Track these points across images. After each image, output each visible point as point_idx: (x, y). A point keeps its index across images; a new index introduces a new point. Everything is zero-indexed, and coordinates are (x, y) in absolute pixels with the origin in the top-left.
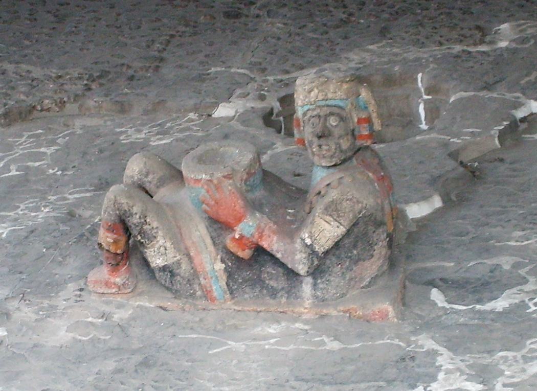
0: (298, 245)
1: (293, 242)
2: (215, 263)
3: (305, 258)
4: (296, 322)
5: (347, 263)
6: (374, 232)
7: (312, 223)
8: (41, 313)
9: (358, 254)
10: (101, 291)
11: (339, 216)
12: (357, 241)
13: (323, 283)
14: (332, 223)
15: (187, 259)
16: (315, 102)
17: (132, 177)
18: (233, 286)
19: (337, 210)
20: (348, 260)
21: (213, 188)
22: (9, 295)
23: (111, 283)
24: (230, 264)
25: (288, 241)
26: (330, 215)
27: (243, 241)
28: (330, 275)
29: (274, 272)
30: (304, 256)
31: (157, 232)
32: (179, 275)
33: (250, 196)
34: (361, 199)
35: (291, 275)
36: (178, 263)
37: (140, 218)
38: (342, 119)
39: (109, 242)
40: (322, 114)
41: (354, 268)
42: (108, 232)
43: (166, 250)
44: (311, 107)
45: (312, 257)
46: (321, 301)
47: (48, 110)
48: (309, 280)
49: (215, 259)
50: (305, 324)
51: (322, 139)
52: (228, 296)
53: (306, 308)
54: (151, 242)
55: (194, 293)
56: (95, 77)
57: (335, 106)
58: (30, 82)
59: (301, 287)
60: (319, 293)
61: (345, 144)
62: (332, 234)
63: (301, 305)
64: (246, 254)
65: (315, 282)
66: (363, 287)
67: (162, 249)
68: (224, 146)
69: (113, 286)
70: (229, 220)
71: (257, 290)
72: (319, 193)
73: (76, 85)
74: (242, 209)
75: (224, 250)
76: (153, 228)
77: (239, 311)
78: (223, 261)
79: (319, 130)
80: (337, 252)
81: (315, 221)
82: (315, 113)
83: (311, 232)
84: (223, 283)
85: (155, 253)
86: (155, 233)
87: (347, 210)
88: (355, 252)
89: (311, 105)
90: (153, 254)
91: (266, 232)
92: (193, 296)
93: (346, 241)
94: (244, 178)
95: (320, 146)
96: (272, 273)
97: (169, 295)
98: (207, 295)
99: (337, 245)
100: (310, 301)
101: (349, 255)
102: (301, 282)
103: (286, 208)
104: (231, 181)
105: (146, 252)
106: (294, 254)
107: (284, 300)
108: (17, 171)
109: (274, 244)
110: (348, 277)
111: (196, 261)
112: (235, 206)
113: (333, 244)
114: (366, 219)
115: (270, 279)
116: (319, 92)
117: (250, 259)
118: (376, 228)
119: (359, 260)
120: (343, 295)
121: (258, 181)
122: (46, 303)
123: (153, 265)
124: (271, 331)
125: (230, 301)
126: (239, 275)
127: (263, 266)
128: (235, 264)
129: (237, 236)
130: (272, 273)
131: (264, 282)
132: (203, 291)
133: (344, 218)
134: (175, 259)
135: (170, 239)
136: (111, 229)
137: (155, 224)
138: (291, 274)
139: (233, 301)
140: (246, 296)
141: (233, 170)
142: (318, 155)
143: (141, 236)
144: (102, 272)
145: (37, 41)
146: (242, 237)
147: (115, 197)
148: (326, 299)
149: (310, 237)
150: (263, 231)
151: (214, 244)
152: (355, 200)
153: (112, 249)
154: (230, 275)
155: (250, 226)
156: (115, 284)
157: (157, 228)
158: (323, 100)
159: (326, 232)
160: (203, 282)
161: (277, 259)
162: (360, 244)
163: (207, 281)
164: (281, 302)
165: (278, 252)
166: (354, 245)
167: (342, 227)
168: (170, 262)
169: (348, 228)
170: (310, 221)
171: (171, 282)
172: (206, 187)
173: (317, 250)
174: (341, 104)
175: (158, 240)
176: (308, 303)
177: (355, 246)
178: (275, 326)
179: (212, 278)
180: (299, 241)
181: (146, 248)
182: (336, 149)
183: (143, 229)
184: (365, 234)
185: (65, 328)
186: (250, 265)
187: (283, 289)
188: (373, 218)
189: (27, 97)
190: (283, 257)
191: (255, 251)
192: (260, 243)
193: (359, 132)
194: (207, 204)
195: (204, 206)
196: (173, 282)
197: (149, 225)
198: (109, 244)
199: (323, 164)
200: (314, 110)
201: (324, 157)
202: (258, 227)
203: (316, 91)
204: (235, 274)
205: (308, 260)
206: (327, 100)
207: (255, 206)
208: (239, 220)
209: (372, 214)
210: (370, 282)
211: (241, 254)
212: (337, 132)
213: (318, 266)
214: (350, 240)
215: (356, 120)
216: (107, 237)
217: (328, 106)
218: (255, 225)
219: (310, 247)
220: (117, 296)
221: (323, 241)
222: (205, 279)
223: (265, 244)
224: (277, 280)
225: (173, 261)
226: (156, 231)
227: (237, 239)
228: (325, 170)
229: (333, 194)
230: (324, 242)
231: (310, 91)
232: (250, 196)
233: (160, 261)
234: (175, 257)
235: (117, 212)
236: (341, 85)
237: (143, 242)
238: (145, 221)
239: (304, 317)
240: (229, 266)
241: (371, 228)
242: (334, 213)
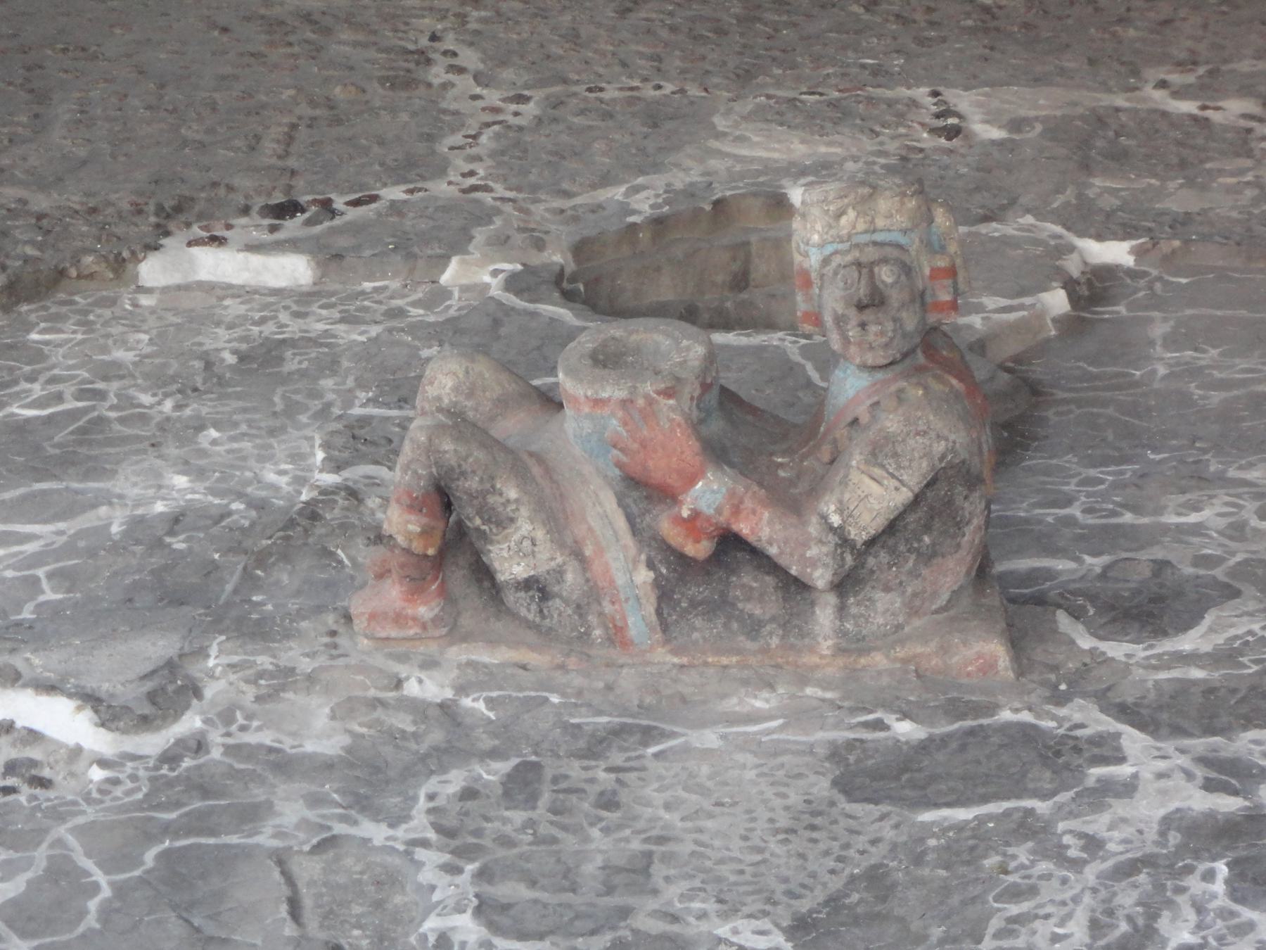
0: (814, 529)
1: (805, 524)
2: (635, 568)
3: (827, 555)
4: (806, 685)
5: (911, 563)
6: (966, 498)
7: (844, 483)
8: (262, 682)
9: (934, 544)
10: (383, 634)
11: (899, 467)
12: (932, 518)
13: (858, 604)
14: (886, 482)
15: (576, 563)
16: (850, 236)
17: (439, 398)
18: (670, 615)
19: (895, 455)
20: (913, 557)
21: (637, 416)
22: (182, 648)
23: (406, 617)
24: (664, 571)
25: (793, 520)
26: (883, 466)
27: (698, 524)
28: (873, 588)
29: (755, 585)
30: (825, 549)
31: (517, 509)
32: (561, 597)
33: (704, 430)
34: (946, 432)
35: (793, 588)
36: (559, 573)
37: (482, 480)
38: (907, 270)
39: (410, 533)
40: (864, 259)
42: (410, 513)
43: (534, 544)
44: (840, 247)
45: (842, 553)
47: (91, 276)
48: (832, 599)
49: (635, 562)
50: (824, 689)
51: (867, 311)
52: (658, 636)
53: (822, 657)
54: (504, 528)
56: (169, 210)
57: (890, 244)
58: (33, 221)
59: (813, 613)
60: (849, 626)
61: (910, 321)
62: (885, 504)
63: (812, 650)
64: (699, 549)
65: (842, 603)
66: (937, 612)
67: (527, 543)
68: (637, 331)
69: (410, 623)
70: (669, 481)
71: (720, 622)
72: (855, 421)
73: (136, 225)
74: (697, 458)
75: (653, 543)
77: (682, 666)
78: (651, 565)
79: (863, 291)
80: (891, 542)
82: (849, 258)
83: (841, 502)
84: (650, 609)
86: (513, 511)
87: (916, 455)
88: (927, 539)
89: (842, 242)
90: (505, 554)
91: (748, 504)
92: (585, 637)
93: (911, 518)
94: (696, 394)
95: (863, 325)
97: (531, 636)
98: (617, 635)
99: (892, 527)
100: (830, 643)
101: (916, 545)
102: (813, 604)
103: (772, 454)
104: (671, 402)
105: (490, 551)
106: (805, 545)
107: (775, 641)
108: (78, 399)
110: (910, 590)
111: (597, 567)
112: (682, 453)
113: (886, 523)
115: (749, 599)
116: (857, 217)
117: (709, 560)
119: (934, 555)
121: (714, 403)
122: (264, 661)
123: (501, 577)
124: (759, 704)
125: (663, 646)
126: (683, 594)
127: (733, 572)
128: (675, 570)
129: (685, 513)
130: (752, 588)
131: (733, 605)
132: (606, 628)
134: (553, 564)
135: (544, 525)
136: (414, 506)
137: (513, 494)
139: (668, 647)
140: (696, 635)
141: (678, 379)
142: (860, 344)
143: (482, 518)
144: (393, 593)
145: (11, 141)
146: (696, 514)
147: (430, 440)
148: (864, 637)
149: (840, 511)
150: (741, 502)
151: (634, 530)
152: (933, 434)
153: (417, 547)
154: (664, 593)
155: (713, 492)
156: (414, 619)
157: (517, 501)
158: (866, 232)
159: (871, 500)
160: (608, 608)
161: (768, 558)
162: (937, 524)
163: (617, 607)
164: (768, 645)
165: (771, 545)
167: (904, 489)
168: (542, 569)
169: (917, 490)
170: (838, 479)
171: (541, 611)
172: (620, 414)
173: (852, 537)
174: (903, 240)
176: (826, 646)
177: (927, 528)
178: (765, 694)
179: (627, 600)
180: (814, 519)
181: (491, 542)
182: (894, 331)
183: (487, 504)
184: (950, 502)
185: (327, 710)
186: (708, 573)
187: (773, 619)
188: (964, 470)
189: (42, 251)
190: (781, 553)
191: (718, 544)
192: (735, 527)
193: (934, 295)
194: (622, 450)
195: (615, 452)
196: (545, 611)
198: (409, 536)
199: (870, 362)
200: (848, 251)
201: (871, 348)
202: (732, 494)
203: (851, 214)
204: (674, 592)
205: (834, 558)
206: (874, 231)
207: (717, 453)
208: (691, 481)
209: (963, 462)
210: (949, 601)
211: (691, 549)
212: (895, 297)
214: (918, 515)
215: (927, 271)
216: (408, 522)
217: (875, 243)
218: (724, 490)
219: (839, 532)
220: (418, 643)
221: (866, 519)
222: (613, 603)
223: (743, 528)
224: (761, 599)
225: (547, 567)
226: (514, 507)
227: (684, 520)
228: (865, 375)
230: (866, 524)
231: (840, 214)
232: (704, 430)
233: (521, 568)
234: (552, 559)
236: (903, 204)
237: (484, 532)
238: (493, 487)
239: (818, 675)
240: (661, 574)
241: (960, 490)
242: (891, 461)
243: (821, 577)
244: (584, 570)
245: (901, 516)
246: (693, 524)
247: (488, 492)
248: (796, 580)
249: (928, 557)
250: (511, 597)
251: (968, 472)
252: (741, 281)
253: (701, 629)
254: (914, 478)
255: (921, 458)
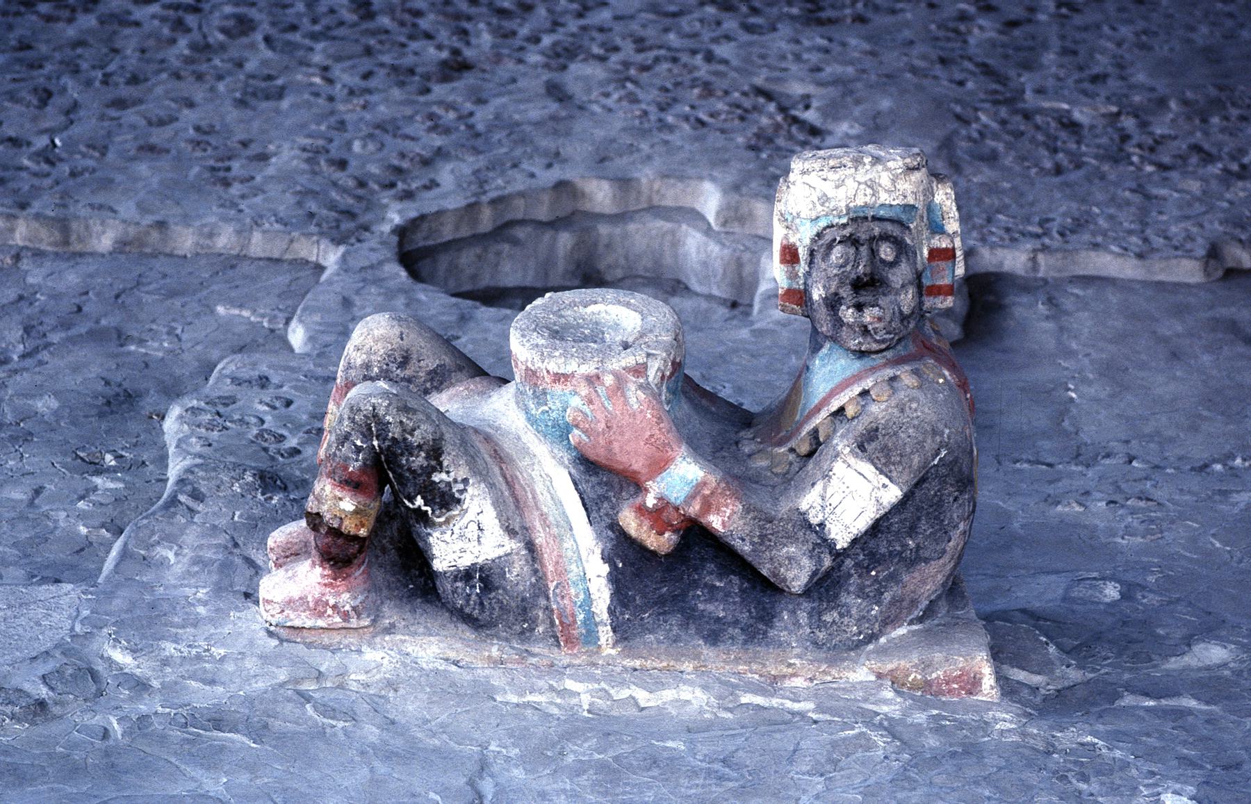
6: (956, 499)
7: (827, 476)
9: (918, 547)
10: (297, 623)
12: (919, 519)
34: (941, 426)
41: (906, 578)
44: (836, 221)
55: (532, 630)
67: (474, 527)
76: (455, 481)
81: (835, 470)
85: (455, 536)
96: (714, 586)
114: (943, 471)
118: (961, 492)
120: (872, 638)
123: (439, 565)
128: (633, 564)
129: (651, 501)
133: (900, 469)
134: (501, 552)
157: (465, 481)
162: (923, 525)
166: (911, 528)
173: (832, 536)
175: (465, 507)
177: (912, 531)
197: (448, 472)
213: (828, 574)
215: (926, 252)
226: (461, 486)
227: (647, 509)
235: (375, 443)
243: (798, 577)
244: (534, 559)
245: (885, 517)
246: (658, 516)
247: (434, 470)
248: (764, 580)
250: (445, 587)
251: (960, 470)
255: (912, 453)
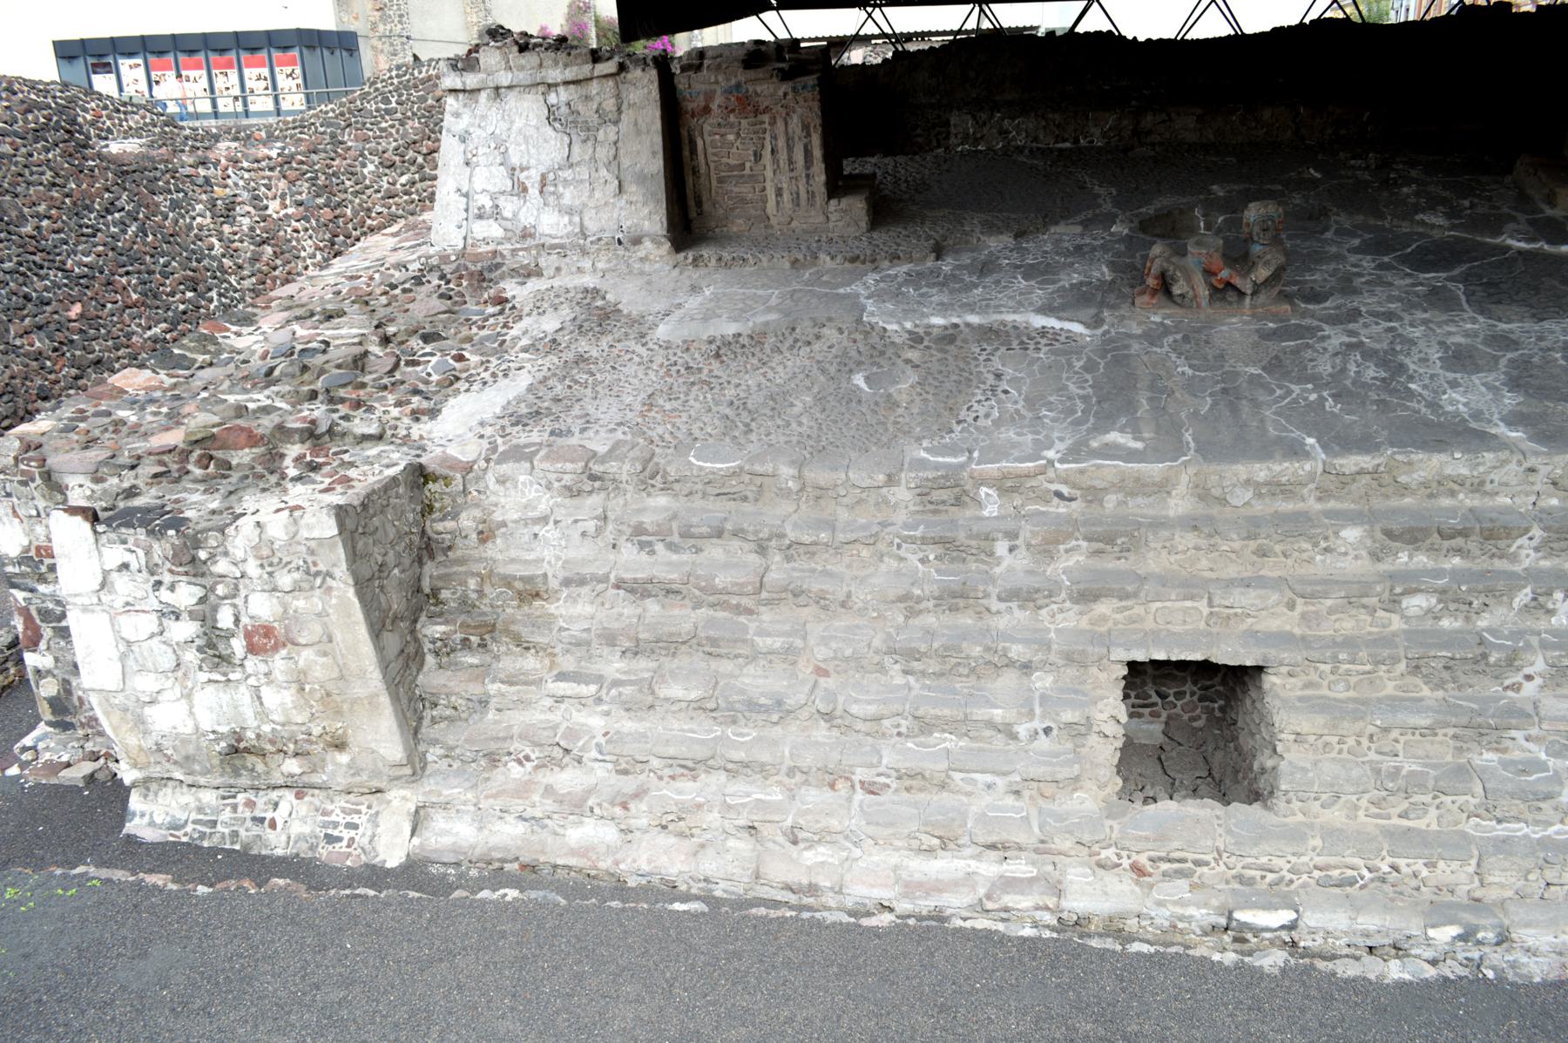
38: (1273, 221)
46: (1253, 307)
99: (1266, 281)
109: (1237, 281)
136: (1156, 278)
138: (1241, 294)
154: (1211, 296)
229: (1269, 257)
230: (1261, 279)
246: (1220, 281)
249: (1273, 287)
252: (1173, 229)
253: (1218, 304)
254: (1272, 269)
